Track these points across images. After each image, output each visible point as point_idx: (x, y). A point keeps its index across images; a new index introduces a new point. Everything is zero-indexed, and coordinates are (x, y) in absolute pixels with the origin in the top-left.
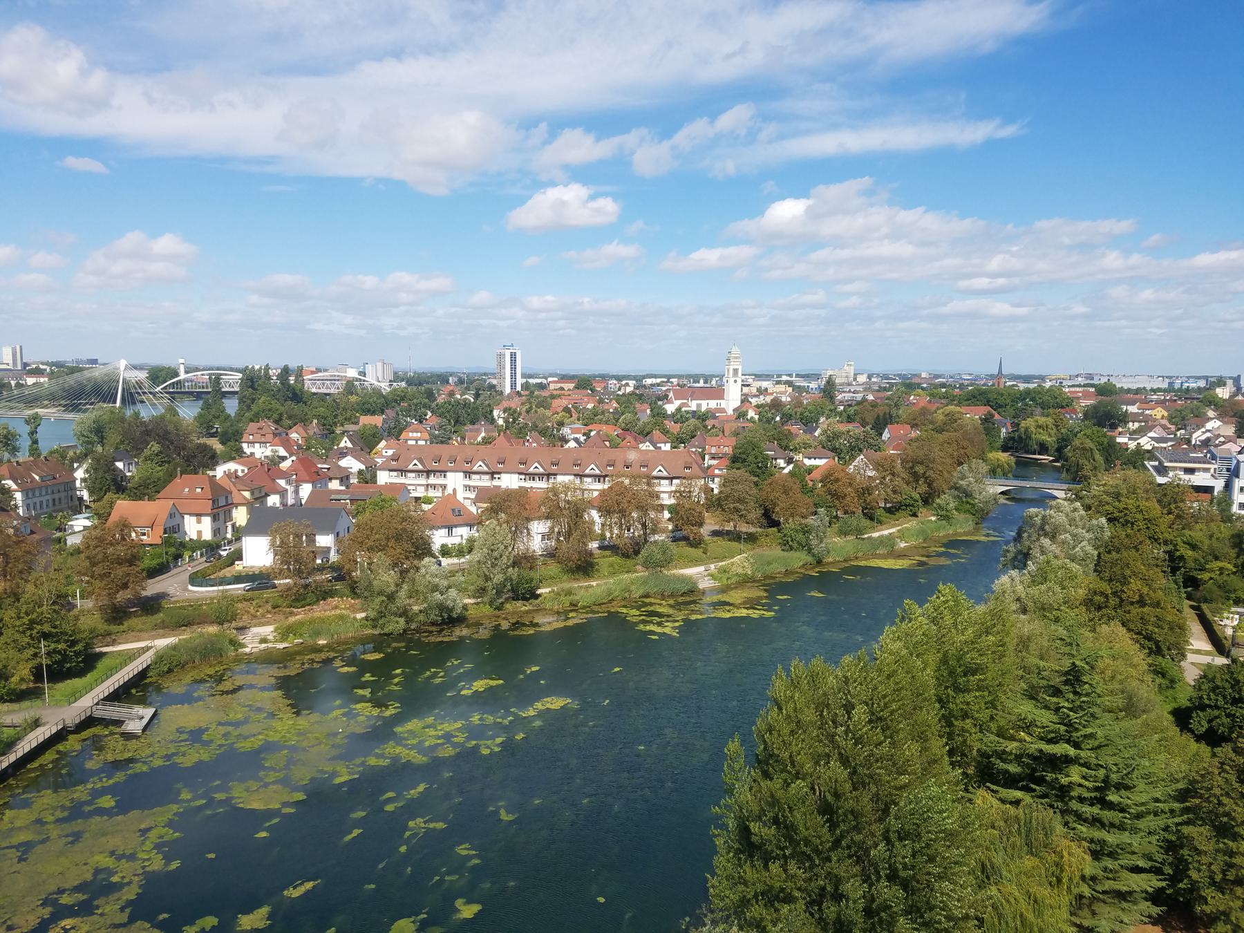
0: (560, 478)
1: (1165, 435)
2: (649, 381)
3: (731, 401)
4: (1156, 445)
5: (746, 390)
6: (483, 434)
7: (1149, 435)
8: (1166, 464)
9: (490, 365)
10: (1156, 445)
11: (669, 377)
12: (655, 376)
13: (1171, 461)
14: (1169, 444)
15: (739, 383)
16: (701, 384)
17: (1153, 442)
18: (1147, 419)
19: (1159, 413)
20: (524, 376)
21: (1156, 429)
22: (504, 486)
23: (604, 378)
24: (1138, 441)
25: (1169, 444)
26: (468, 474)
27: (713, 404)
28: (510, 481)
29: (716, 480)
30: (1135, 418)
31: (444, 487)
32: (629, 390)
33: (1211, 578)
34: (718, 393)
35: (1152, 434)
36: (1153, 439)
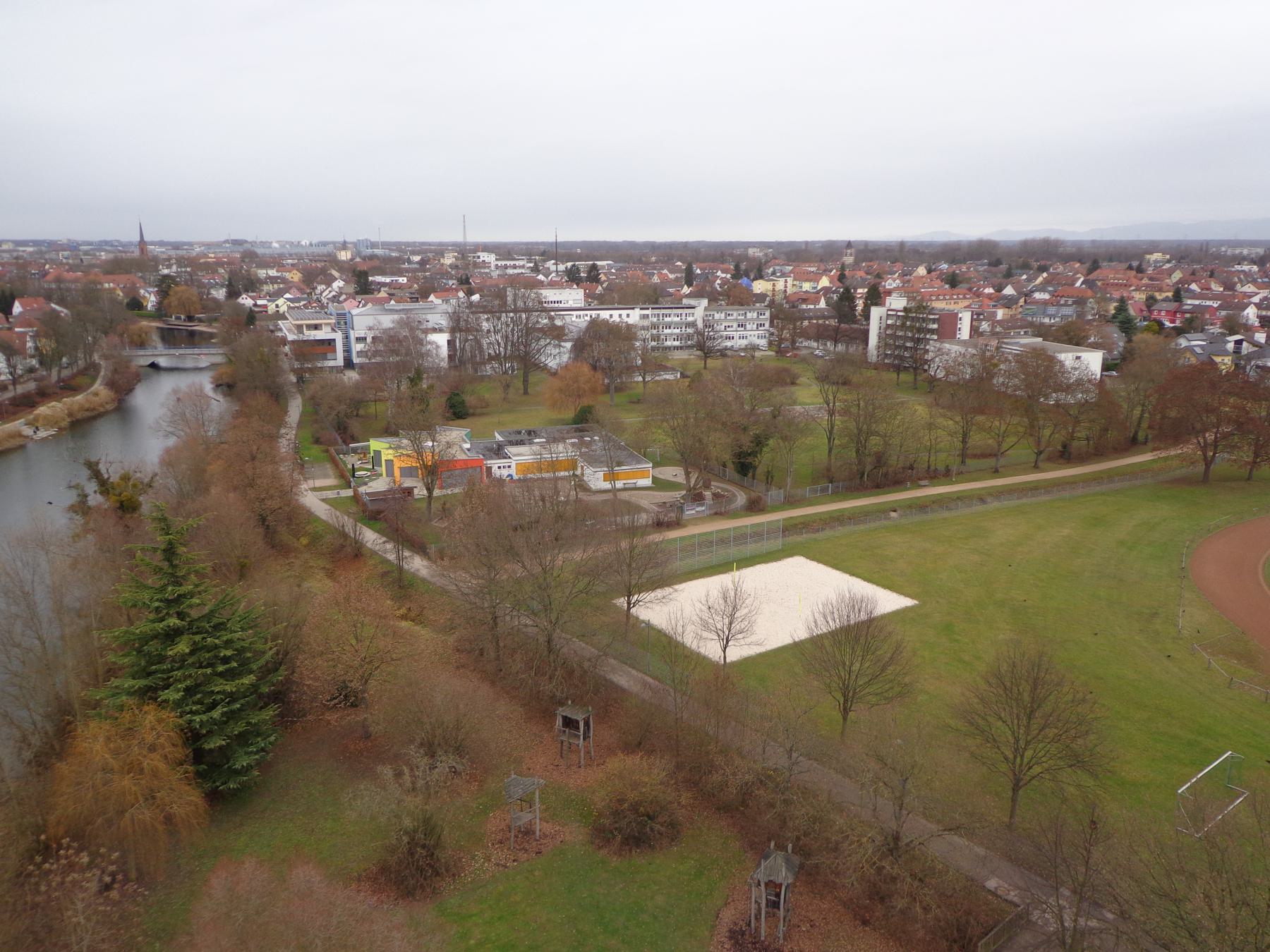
1: (299, 295)
4: (292, 305)
7: (285, 296)
10: (292, 305)
13: (297, 320)
14: (302, 303)
17: (289, 303)
18: (284, 280)
19: (295, 276)
21: (292, 291)
24: (277, 303)
25: (302, 303)
30: (273, 280)
35: (287, 296)
36: (288, 299)
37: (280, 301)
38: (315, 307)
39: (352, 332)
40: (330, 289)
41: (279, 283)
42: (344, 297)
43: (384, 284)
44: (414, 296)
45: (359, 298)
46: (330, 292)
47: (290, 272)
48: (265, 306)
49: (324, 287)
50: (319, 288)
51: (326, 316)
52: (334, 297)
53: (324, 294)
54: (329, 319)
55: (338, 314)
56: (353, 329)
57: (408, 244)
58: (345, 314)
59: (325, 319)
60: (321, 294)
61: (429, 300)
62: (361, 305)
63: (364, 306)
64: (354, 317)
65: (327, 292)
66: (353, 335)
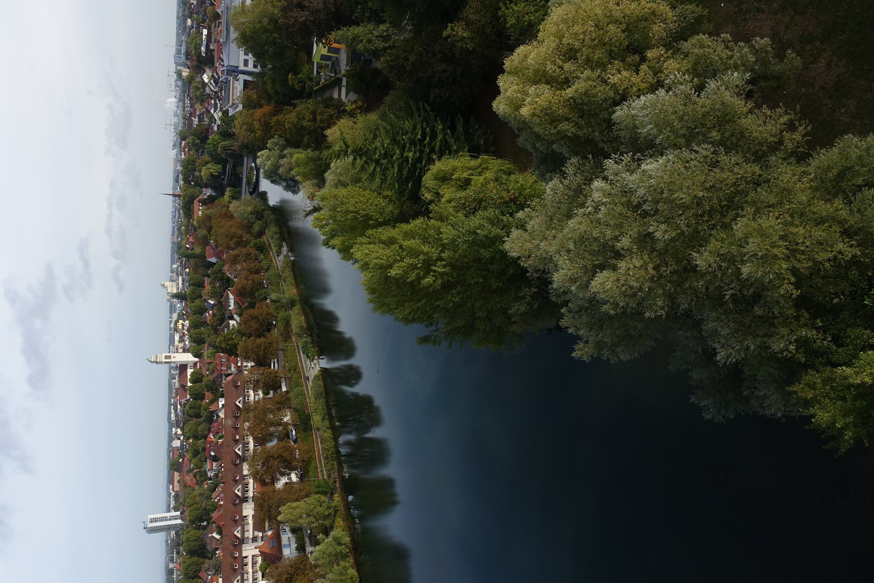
0: (245, 472)
2: (173, 415)
3: (189, 358)
5: (180, 350)
6: (215, 535)
8: (231, 104)
9: (161, 536)
11: (170, 405)
12: (170, 413)
13: (229, 101)
14: (218, 102)
15: (175, 355)
16: (176, 381)
17: (217, 111)
20: (169, 511)
22: (253, 512)
23: (171, 449)
25: (218, 102)
26: (242, 541)
27: (190, 371)
28: (248, 510)
29: (245, 364)
30: (201, 120)
31: (253, 556)
32: (179, 432)
33: (298, 84)
34: (183, 368)
35: (212, 111)
36: (215, 111)
37: (215, 115)
38: (221, 93)
39: (240, 68)
40: (209, 84)
41: (203, 116)
42: (215, 74)
43: (207, 46)
44: (217, 25)
45: (217, 65)
46: (211, 84)
47: (196, 110)
48: (218, 126)
49: (207, 88)
50: (208, 92)
51: (228, 82)
52: (214, 82)
53: (213, 89)
54: (230, 81)
55: (227, 75)
56: (238, 67)
57: (178, 28)
58: (227, 70)
59: (230, 84)
60: (212, 90)
61: (220, 13)
62: (222, 63)
63: (223, 61)
64: (230, 64)
65: (211, 86)
66: (242, 67)
